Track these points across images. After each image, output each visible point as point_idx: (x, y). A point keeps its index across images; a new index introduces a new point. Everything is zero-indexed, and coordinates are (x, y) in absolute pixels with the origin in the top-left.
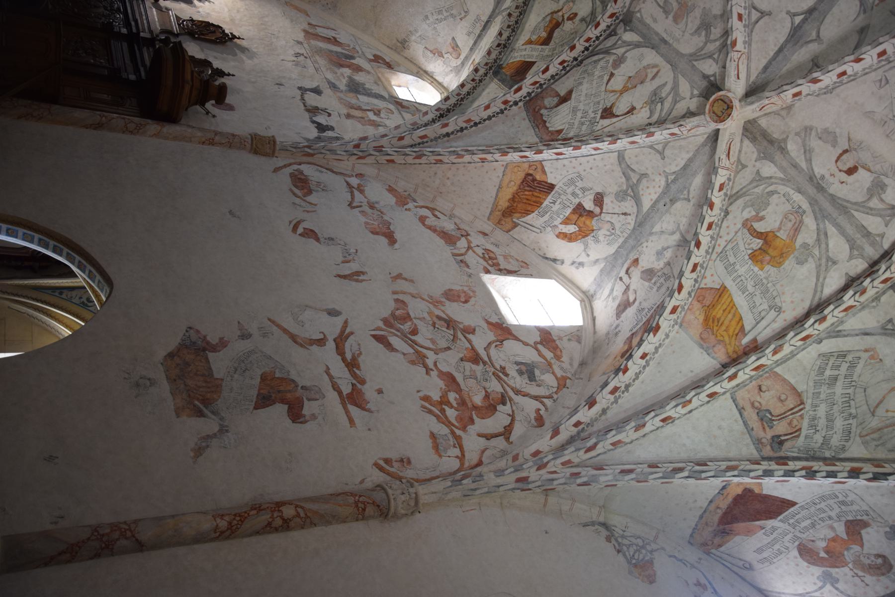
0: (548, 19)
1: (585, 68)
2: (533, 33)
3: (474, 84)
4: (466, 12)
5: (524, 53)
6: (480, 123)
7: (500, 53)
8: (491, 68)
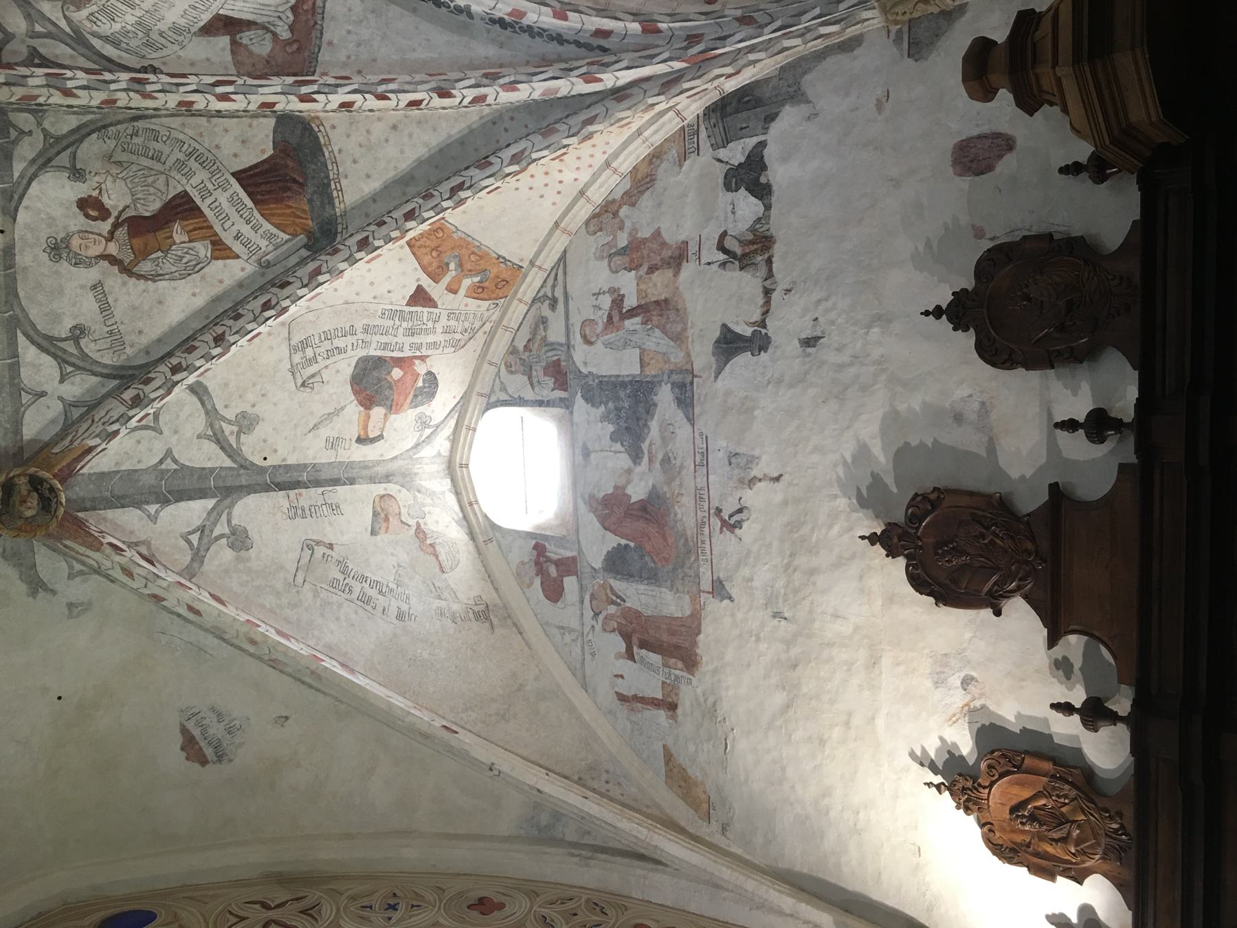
0: (145, 267)
1: (146, 51)
2: (194, 268)
5: (246, 230)
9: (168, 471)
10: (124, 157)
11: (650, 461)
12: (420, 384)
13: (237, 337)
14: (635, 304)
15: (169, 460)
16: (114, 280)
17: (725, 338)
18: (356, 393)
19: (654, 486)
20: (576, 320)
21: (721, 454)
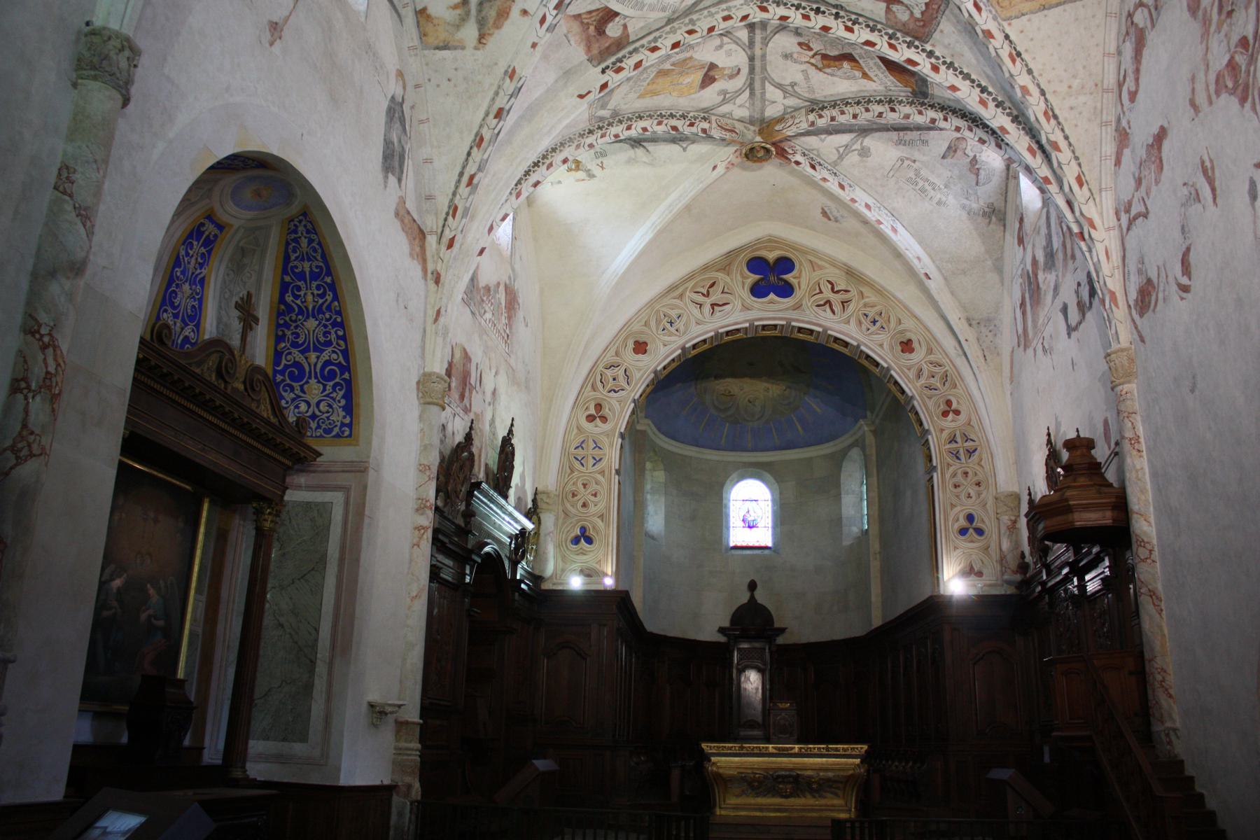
2: (854, 78)
3: (950, 116)
4: (902, 161)
6: (979, 86)
7: (900, 102)
8: (923, 104)
16: (812, 72)
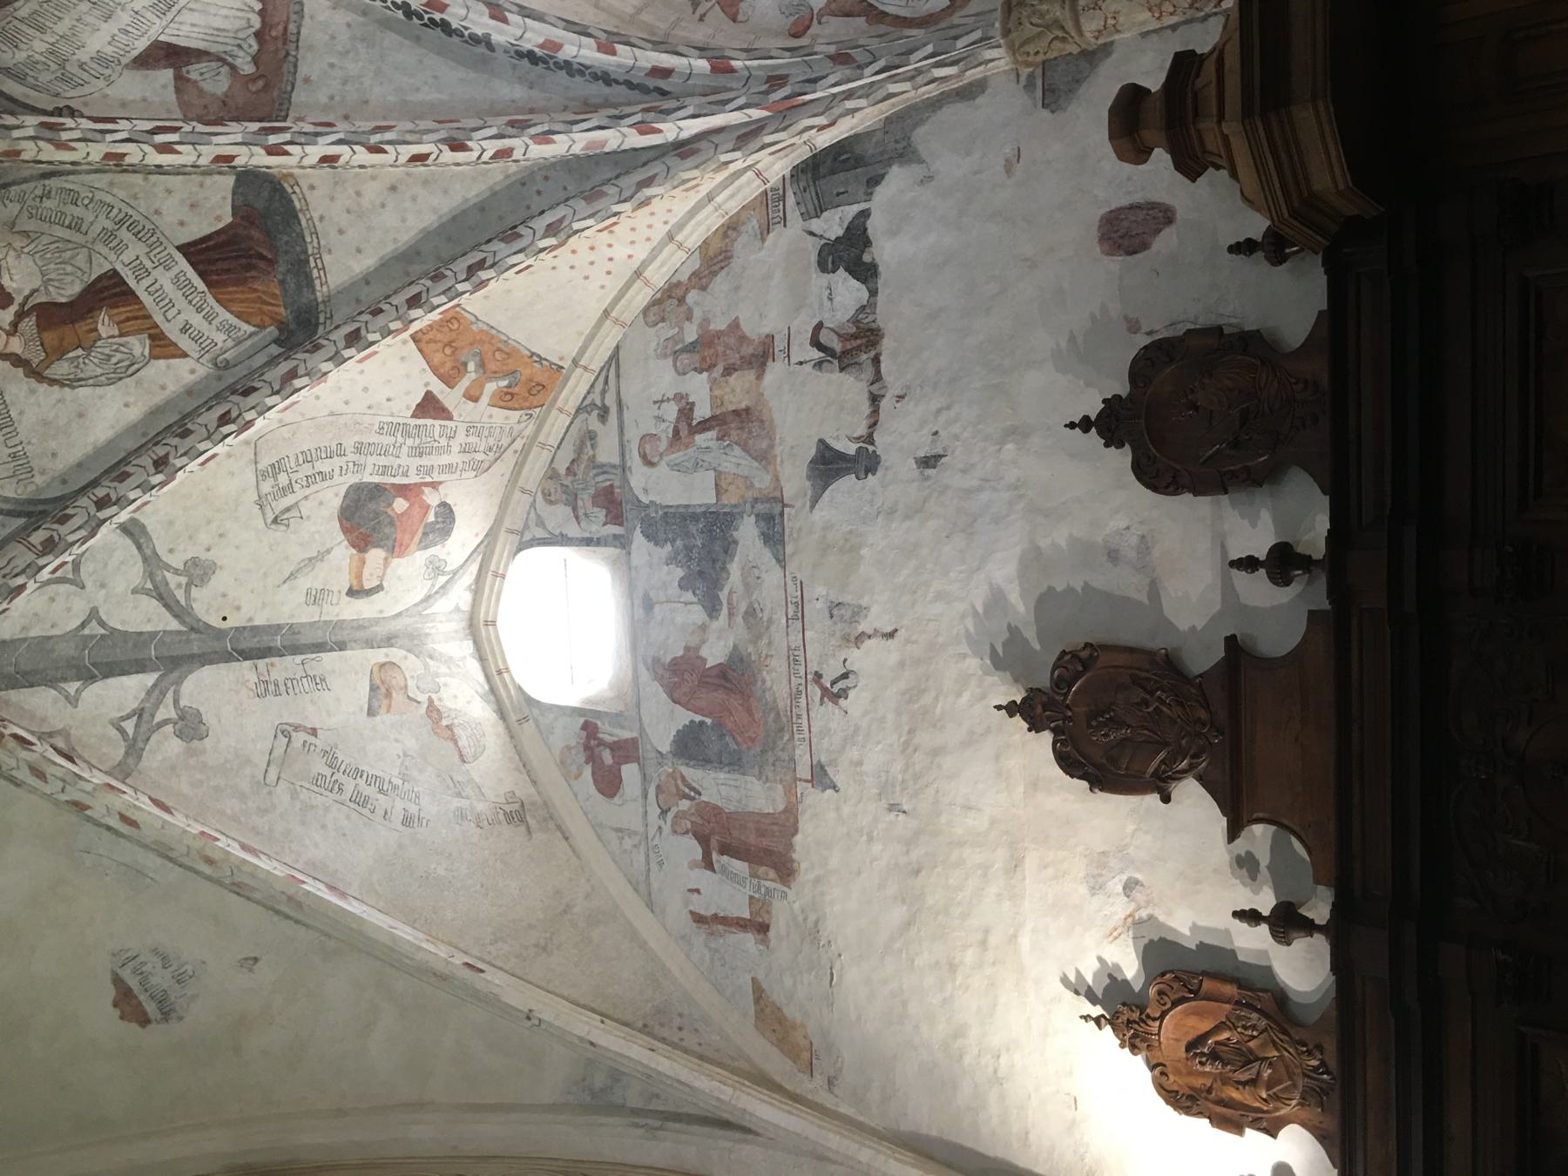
0: (61, 369)
1: (59, 87)
5: (197, 320)
9: (92, 637)
10: (31, 226)
11: (731, 614)
12: (431, 518)
13: (185, 460)
14: (708, 414)
15: (94, 623)
17: (823, 457)
18: (345, 531)
19: (735, 647)
20: (633, 435)
21: (819, 605)
